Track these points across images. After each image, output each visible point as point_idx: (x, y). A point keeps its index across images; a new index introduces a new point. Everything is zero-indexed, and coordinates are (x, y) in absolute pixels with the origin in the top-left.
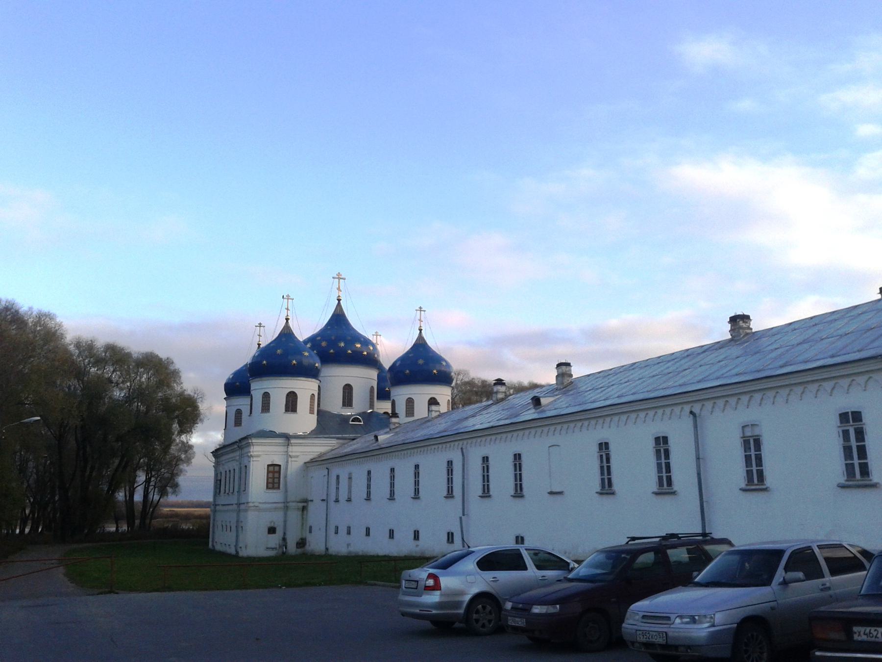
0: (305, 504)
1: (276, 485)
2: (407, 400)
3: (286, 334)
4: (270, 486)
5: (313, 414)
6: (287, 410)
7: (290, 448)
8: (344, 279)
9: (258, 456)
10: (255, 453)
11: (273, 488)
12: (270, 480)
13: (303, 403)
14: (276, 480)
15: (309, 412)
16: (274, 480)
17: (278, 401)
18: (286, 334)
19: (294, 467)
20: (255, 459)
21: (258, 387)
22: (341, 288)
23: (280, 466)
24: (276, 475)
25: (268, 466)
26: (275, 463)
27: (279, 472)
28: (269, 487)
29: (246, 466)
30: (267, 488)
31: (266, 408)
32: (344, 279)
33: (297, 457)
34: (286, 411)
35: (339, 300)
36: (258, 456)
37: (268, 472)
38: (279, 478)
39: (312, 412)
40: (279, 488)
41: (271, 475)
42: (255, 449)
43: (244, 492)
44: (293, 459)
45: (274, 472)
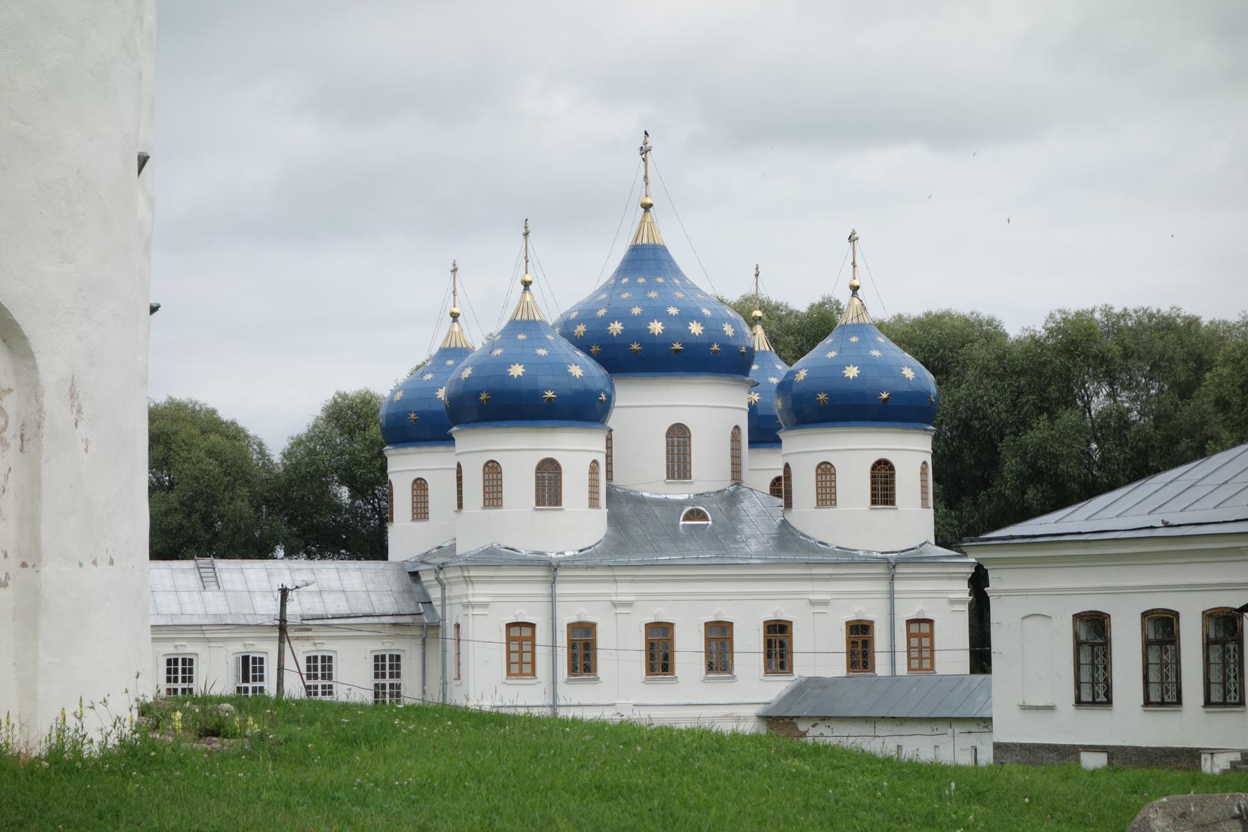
1: (527, 669)
2: (819, 466)
4: (515, 669)
6: (540, 501)
9: (485, 605)
10: (477, 599)
11: (521, 674)
12: (515, 657)
13: (574, 483)
14: (527, 657)
16: (521, 657)
20: (477, 611)
23: (532, 626)
24: (527, 647)
25: (509, 626)
26: (520, 620)
28: (512, 672)
29: (458, 626)
30: (509, 674)
31: (493, 496)
34: (538, 504)
37: (509, 640)
38: (533, 653)
40: (533, 673)
41: (515, 647)
42: (476, 592)
43: (458, 682)
45: (521, 640)
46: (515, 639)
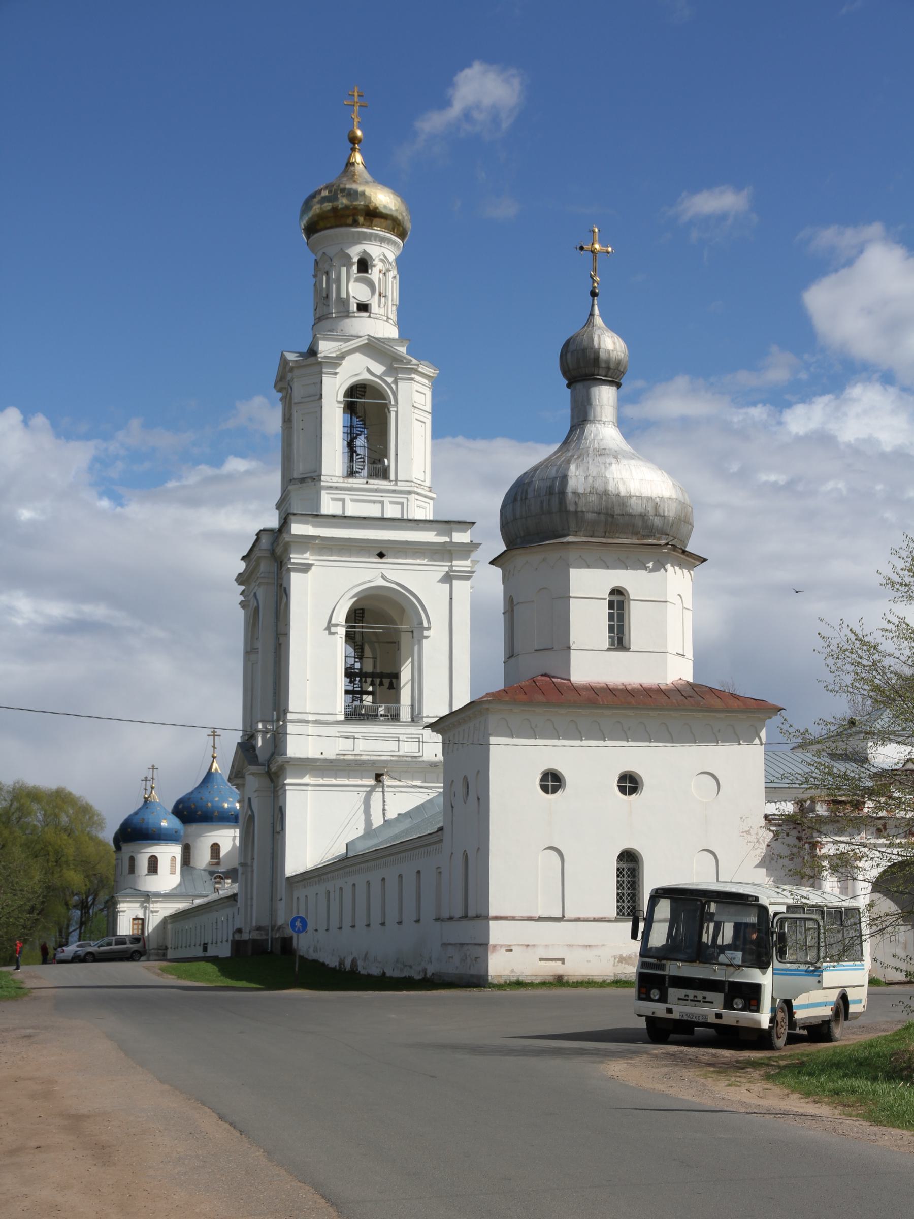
0: (165, 951)
5: (175, 874)
8: (219, 736)
9: (124, 911)
10: (121, 909)
13: (163, 865)
15: (169, 872)
19: (153, 922)
20: (121, 914)
22: (216, 746)
25: (134, 919)
32: (219, 736)
33: (157, 912)
36: (124, 911)
37: (133, 924)
39: (173, 872)
44: (154, 914)
46: (135, 924)
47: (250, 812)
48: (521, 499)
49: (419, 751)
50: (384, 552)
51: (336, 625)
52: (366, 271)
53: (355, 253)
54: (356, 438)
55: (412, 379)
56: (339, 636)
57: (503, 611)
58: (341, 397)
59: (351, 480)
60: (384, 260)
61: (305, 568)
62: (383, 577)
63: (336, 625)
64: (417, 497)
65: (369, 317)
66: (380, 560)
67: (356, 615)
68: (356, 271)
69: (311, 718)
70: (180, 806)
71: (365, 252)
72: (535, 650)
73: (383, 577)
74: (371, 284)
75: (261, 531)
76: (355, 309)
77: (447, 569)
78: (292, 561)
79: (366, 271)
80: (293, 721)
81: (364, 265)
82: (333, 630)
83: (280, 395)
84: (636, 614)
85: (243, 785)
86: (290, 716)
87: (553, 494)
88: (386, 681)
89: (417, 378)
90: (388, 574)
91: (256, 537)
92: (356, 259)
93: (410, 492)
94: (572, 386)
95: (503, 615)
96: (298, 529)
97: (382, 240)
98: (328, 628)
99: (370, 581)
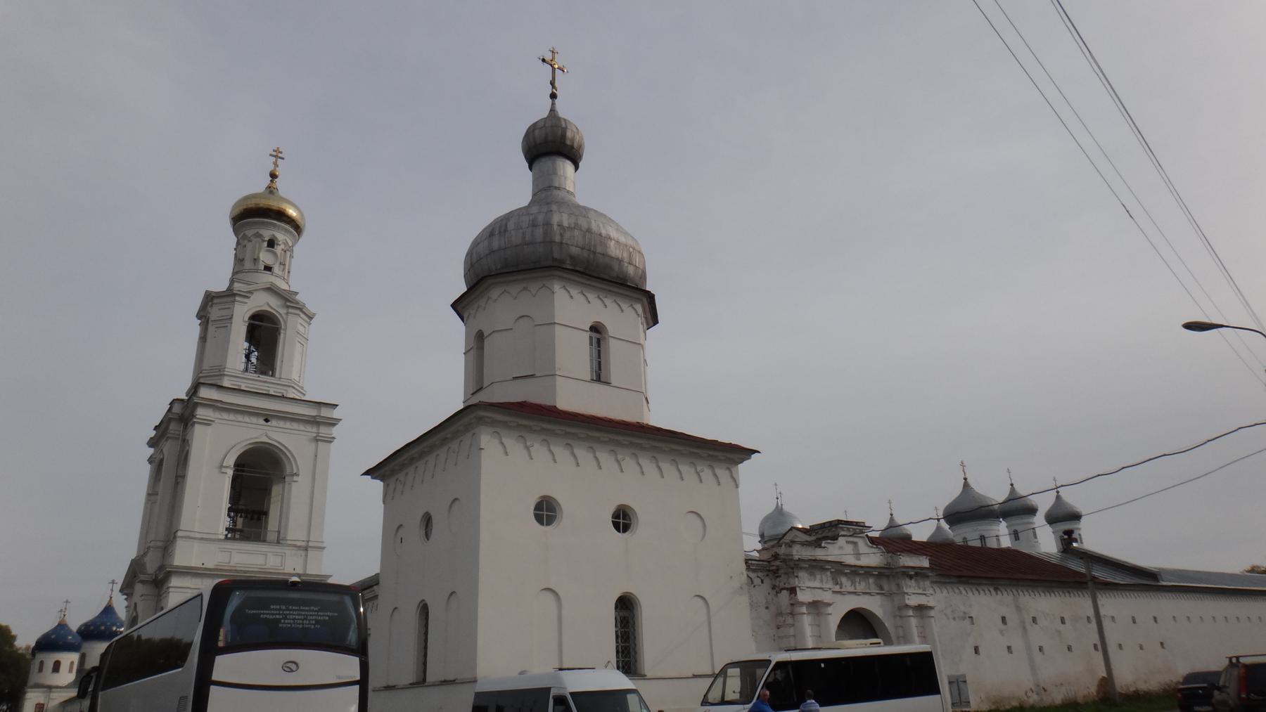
3: (62, 626)
7: (51, 694)
13: (64, 667)
17: (49, 665)
18: (62, 626)
21: (40, 656)
27: (43, 707)
31: (41, 670)
35: (111, 598)
39: (70, 671)
47: (134, 614)
48: (500, 232)
49: (282, 566)
50: (269, 419)
51: (227, 467)
52: (273, 247)
53: (267, 234)
54: (252, 353)
55: (299, 315)
56: (227, 476)
57: (464, 351)
58: (246, 319)
59: (246, 374)
60: (286, 243)
61: (207, 423)
62: (267, 436)
63: (227, 467)
64: (294, 390)
65: (272, 275)
66: (266, 424)
67: (240, 465)
68: (266, 245)
69: (198, 536)
70: (83, 628)
71: (274, 235)
72: (514, 378)
73: (267, 436)
74: (275, 254)
75: (174, 400)
76: (263, 269)
77: (315, 435)
78: (198, 417)
79: (273, 247)
80: (182, 537)
81: (272, 243)
82: (224, 470)
83: (199, 321)
84: (615, 349)
85: (132, 594)
86: (179, 534)
87: (536, 226)
88: (256, 516)
89: (302, 315)
90: (271, 434)
91: (169, 406)
92: (267, 239)
93: (289, 386)
94: (536, 166)
95: (463, 355)
96: (205, 393)
97: (286, 230)
98: (221, 466)
99: (256, 438)
